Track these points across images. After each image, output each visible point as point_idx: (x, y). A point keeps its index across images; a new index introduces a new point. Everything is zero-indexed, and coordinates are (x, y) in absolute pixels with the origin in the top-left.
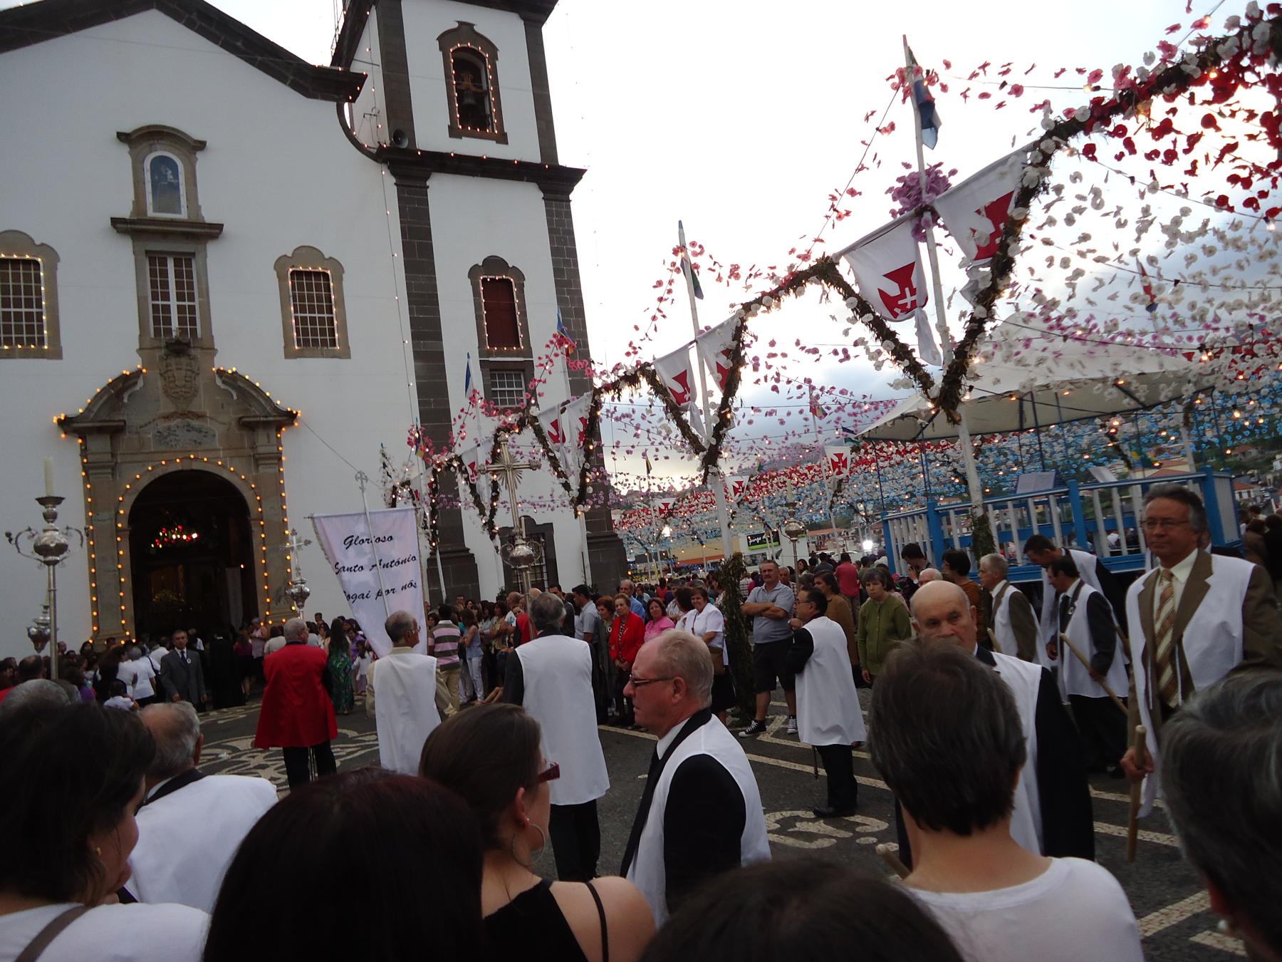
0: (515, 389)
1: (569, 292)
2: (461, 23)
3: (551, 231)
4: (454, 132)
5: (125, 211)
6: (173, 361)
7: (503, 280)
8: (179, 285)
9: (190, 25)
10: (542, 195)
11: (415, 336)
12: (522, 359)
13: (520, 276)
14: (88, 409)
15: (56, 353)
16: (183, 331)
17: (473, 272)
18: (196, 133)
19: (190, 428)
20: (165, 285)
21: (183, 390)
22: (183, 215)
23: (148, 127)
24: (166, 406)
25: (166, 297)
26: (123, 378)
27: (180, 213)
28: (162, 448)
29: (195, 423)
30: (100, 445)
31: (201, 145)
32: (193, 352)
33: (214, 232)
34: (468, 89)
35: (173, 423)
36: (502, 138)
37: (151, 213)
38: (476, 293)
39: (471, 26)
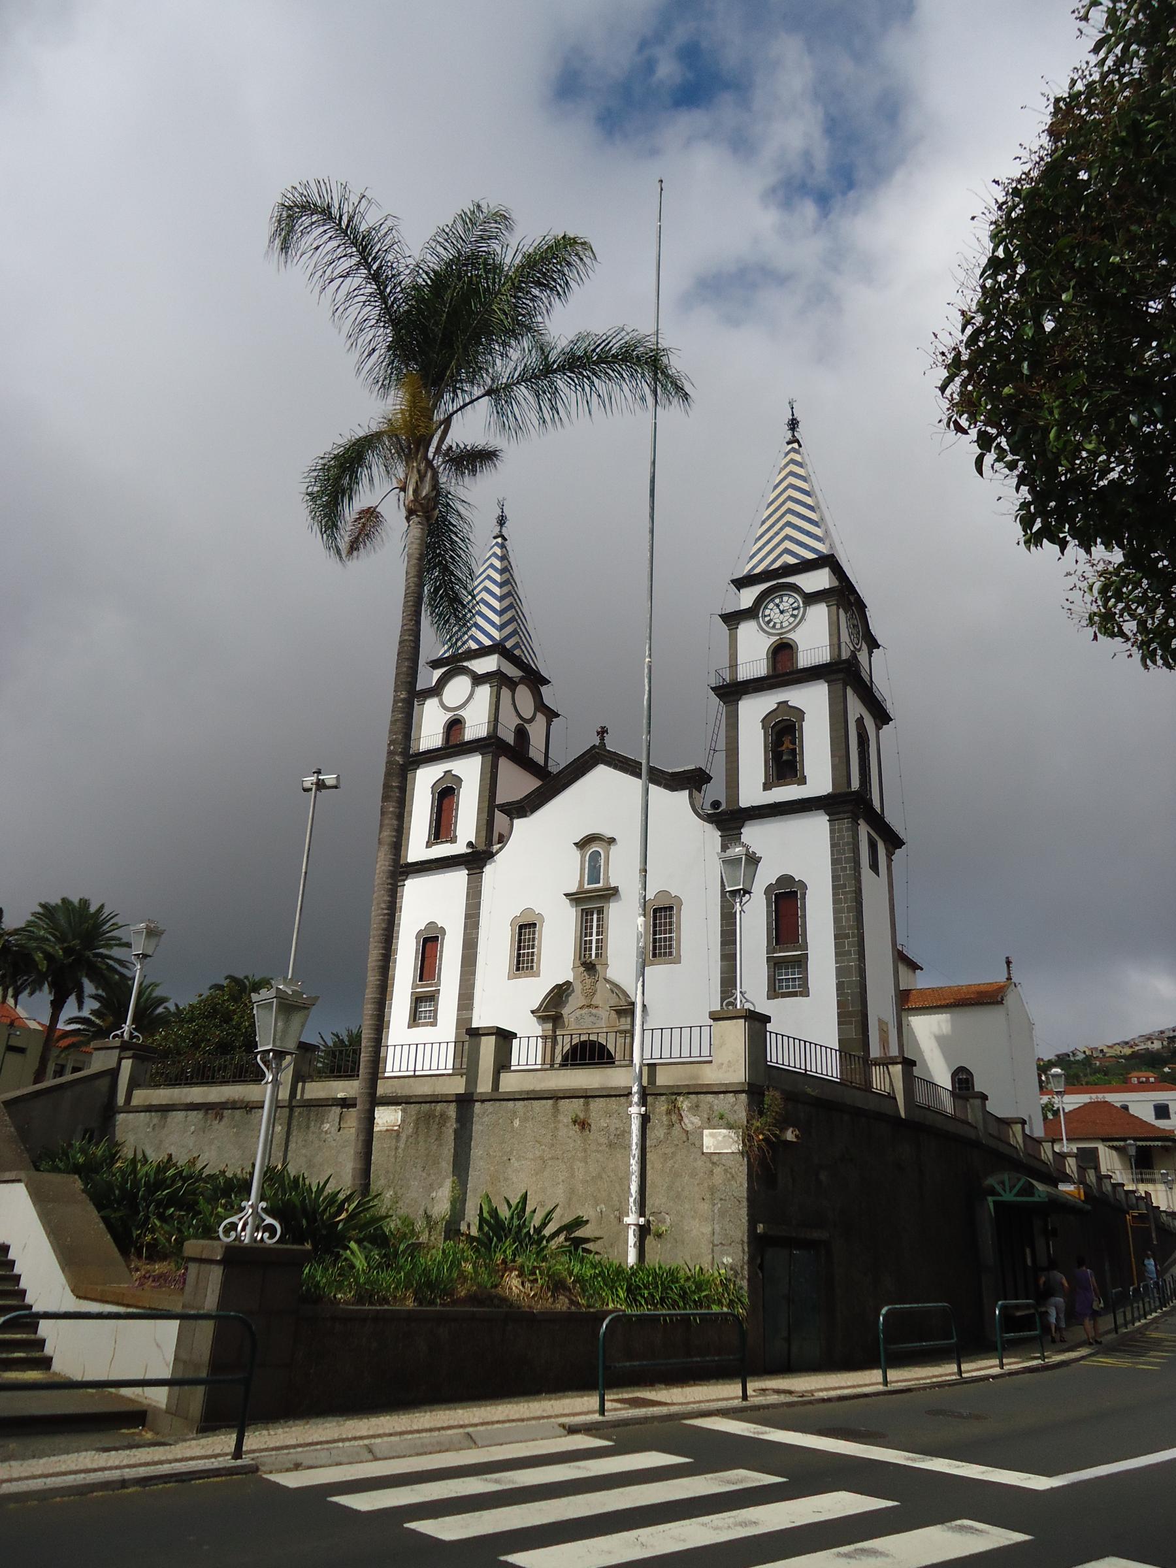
0: (796, 976)
1: (844, 893)
2: (779, 703)
3: (832, 846)
4: (767, 786)
5: (574, 890)
6: (585, 973)
7: (791, 891)
8: (598, 927)
9: (615, 767)
10: (828, 818)
11: (723, 944)
12: (799, 953)
13: (803, 886)
14: (541, 1005)
15: (539, 976)
16: (597, 955)
17: (768, 890)
18: (609, 834)
19: (591, 1014)
20: (591, 928)
21: (590, 991)
22: (600, 885)
23: (587, 836)
24: (582, 1001)
25: (591, 936)
26: (558, 986)
27: (599, 883)
28: (578, 1027)
29: (594, 1011)
30: (549, 1026)
31: (612, 841)
32: (598, 967)
33: (615, 891)
34: (787, 748)
35: (585, 1011)
36: (802, 781)
37: (586, 886)
38: (769, 905)
39: (786, 702)
